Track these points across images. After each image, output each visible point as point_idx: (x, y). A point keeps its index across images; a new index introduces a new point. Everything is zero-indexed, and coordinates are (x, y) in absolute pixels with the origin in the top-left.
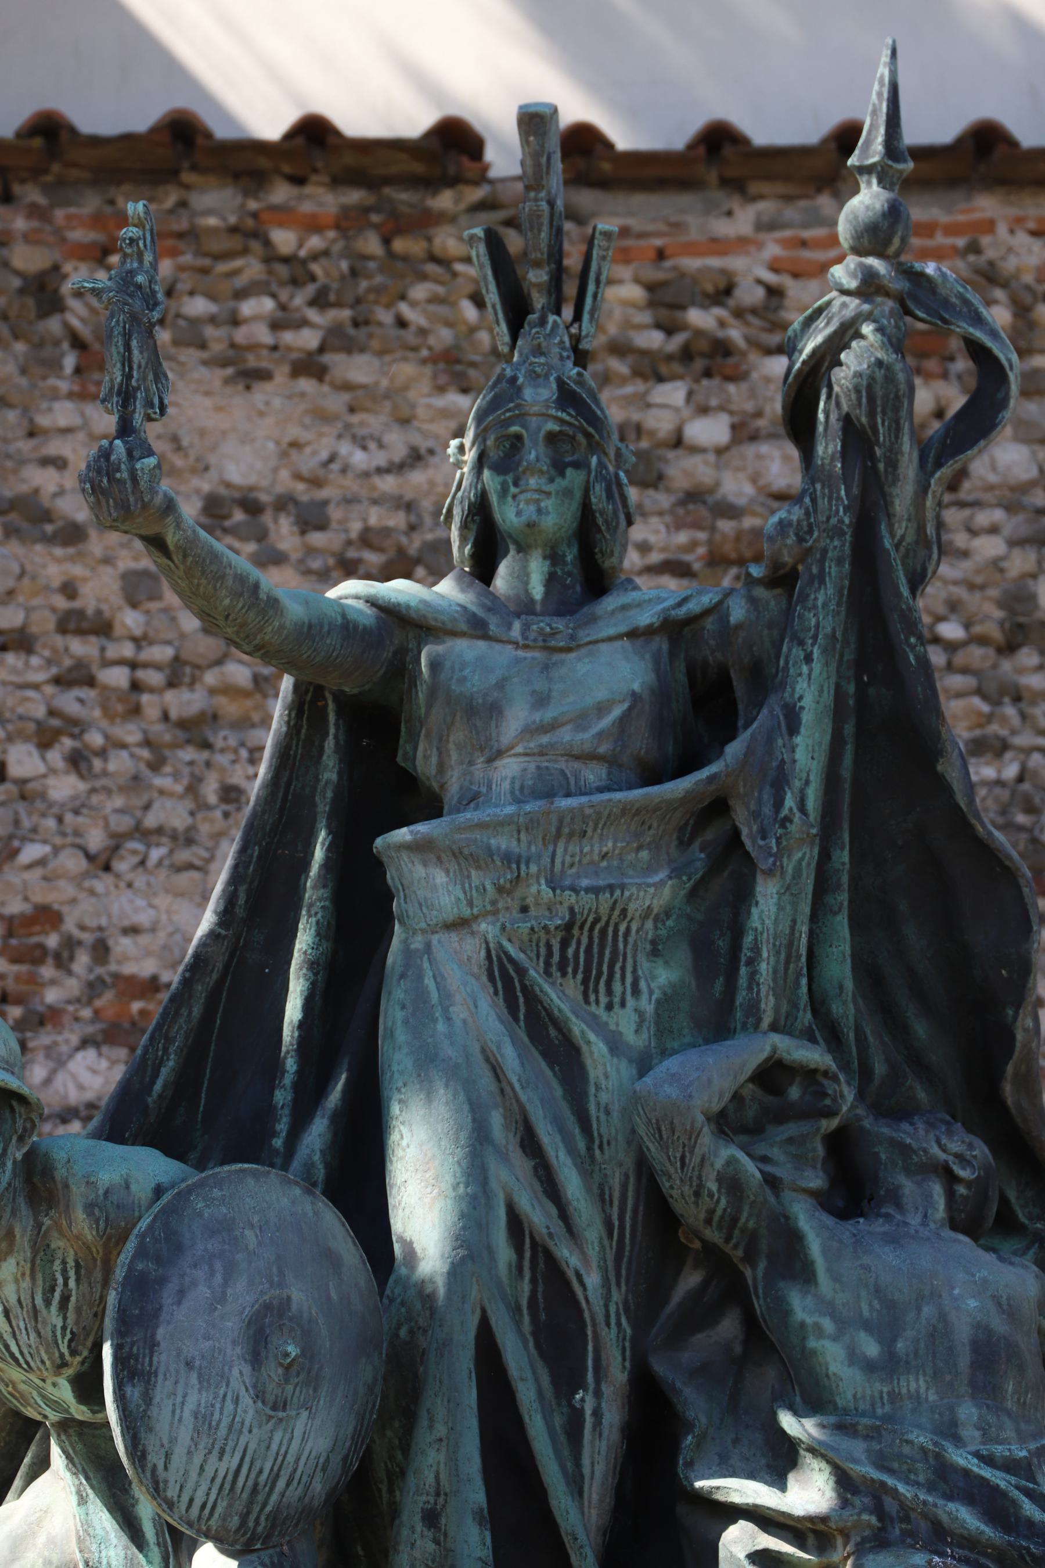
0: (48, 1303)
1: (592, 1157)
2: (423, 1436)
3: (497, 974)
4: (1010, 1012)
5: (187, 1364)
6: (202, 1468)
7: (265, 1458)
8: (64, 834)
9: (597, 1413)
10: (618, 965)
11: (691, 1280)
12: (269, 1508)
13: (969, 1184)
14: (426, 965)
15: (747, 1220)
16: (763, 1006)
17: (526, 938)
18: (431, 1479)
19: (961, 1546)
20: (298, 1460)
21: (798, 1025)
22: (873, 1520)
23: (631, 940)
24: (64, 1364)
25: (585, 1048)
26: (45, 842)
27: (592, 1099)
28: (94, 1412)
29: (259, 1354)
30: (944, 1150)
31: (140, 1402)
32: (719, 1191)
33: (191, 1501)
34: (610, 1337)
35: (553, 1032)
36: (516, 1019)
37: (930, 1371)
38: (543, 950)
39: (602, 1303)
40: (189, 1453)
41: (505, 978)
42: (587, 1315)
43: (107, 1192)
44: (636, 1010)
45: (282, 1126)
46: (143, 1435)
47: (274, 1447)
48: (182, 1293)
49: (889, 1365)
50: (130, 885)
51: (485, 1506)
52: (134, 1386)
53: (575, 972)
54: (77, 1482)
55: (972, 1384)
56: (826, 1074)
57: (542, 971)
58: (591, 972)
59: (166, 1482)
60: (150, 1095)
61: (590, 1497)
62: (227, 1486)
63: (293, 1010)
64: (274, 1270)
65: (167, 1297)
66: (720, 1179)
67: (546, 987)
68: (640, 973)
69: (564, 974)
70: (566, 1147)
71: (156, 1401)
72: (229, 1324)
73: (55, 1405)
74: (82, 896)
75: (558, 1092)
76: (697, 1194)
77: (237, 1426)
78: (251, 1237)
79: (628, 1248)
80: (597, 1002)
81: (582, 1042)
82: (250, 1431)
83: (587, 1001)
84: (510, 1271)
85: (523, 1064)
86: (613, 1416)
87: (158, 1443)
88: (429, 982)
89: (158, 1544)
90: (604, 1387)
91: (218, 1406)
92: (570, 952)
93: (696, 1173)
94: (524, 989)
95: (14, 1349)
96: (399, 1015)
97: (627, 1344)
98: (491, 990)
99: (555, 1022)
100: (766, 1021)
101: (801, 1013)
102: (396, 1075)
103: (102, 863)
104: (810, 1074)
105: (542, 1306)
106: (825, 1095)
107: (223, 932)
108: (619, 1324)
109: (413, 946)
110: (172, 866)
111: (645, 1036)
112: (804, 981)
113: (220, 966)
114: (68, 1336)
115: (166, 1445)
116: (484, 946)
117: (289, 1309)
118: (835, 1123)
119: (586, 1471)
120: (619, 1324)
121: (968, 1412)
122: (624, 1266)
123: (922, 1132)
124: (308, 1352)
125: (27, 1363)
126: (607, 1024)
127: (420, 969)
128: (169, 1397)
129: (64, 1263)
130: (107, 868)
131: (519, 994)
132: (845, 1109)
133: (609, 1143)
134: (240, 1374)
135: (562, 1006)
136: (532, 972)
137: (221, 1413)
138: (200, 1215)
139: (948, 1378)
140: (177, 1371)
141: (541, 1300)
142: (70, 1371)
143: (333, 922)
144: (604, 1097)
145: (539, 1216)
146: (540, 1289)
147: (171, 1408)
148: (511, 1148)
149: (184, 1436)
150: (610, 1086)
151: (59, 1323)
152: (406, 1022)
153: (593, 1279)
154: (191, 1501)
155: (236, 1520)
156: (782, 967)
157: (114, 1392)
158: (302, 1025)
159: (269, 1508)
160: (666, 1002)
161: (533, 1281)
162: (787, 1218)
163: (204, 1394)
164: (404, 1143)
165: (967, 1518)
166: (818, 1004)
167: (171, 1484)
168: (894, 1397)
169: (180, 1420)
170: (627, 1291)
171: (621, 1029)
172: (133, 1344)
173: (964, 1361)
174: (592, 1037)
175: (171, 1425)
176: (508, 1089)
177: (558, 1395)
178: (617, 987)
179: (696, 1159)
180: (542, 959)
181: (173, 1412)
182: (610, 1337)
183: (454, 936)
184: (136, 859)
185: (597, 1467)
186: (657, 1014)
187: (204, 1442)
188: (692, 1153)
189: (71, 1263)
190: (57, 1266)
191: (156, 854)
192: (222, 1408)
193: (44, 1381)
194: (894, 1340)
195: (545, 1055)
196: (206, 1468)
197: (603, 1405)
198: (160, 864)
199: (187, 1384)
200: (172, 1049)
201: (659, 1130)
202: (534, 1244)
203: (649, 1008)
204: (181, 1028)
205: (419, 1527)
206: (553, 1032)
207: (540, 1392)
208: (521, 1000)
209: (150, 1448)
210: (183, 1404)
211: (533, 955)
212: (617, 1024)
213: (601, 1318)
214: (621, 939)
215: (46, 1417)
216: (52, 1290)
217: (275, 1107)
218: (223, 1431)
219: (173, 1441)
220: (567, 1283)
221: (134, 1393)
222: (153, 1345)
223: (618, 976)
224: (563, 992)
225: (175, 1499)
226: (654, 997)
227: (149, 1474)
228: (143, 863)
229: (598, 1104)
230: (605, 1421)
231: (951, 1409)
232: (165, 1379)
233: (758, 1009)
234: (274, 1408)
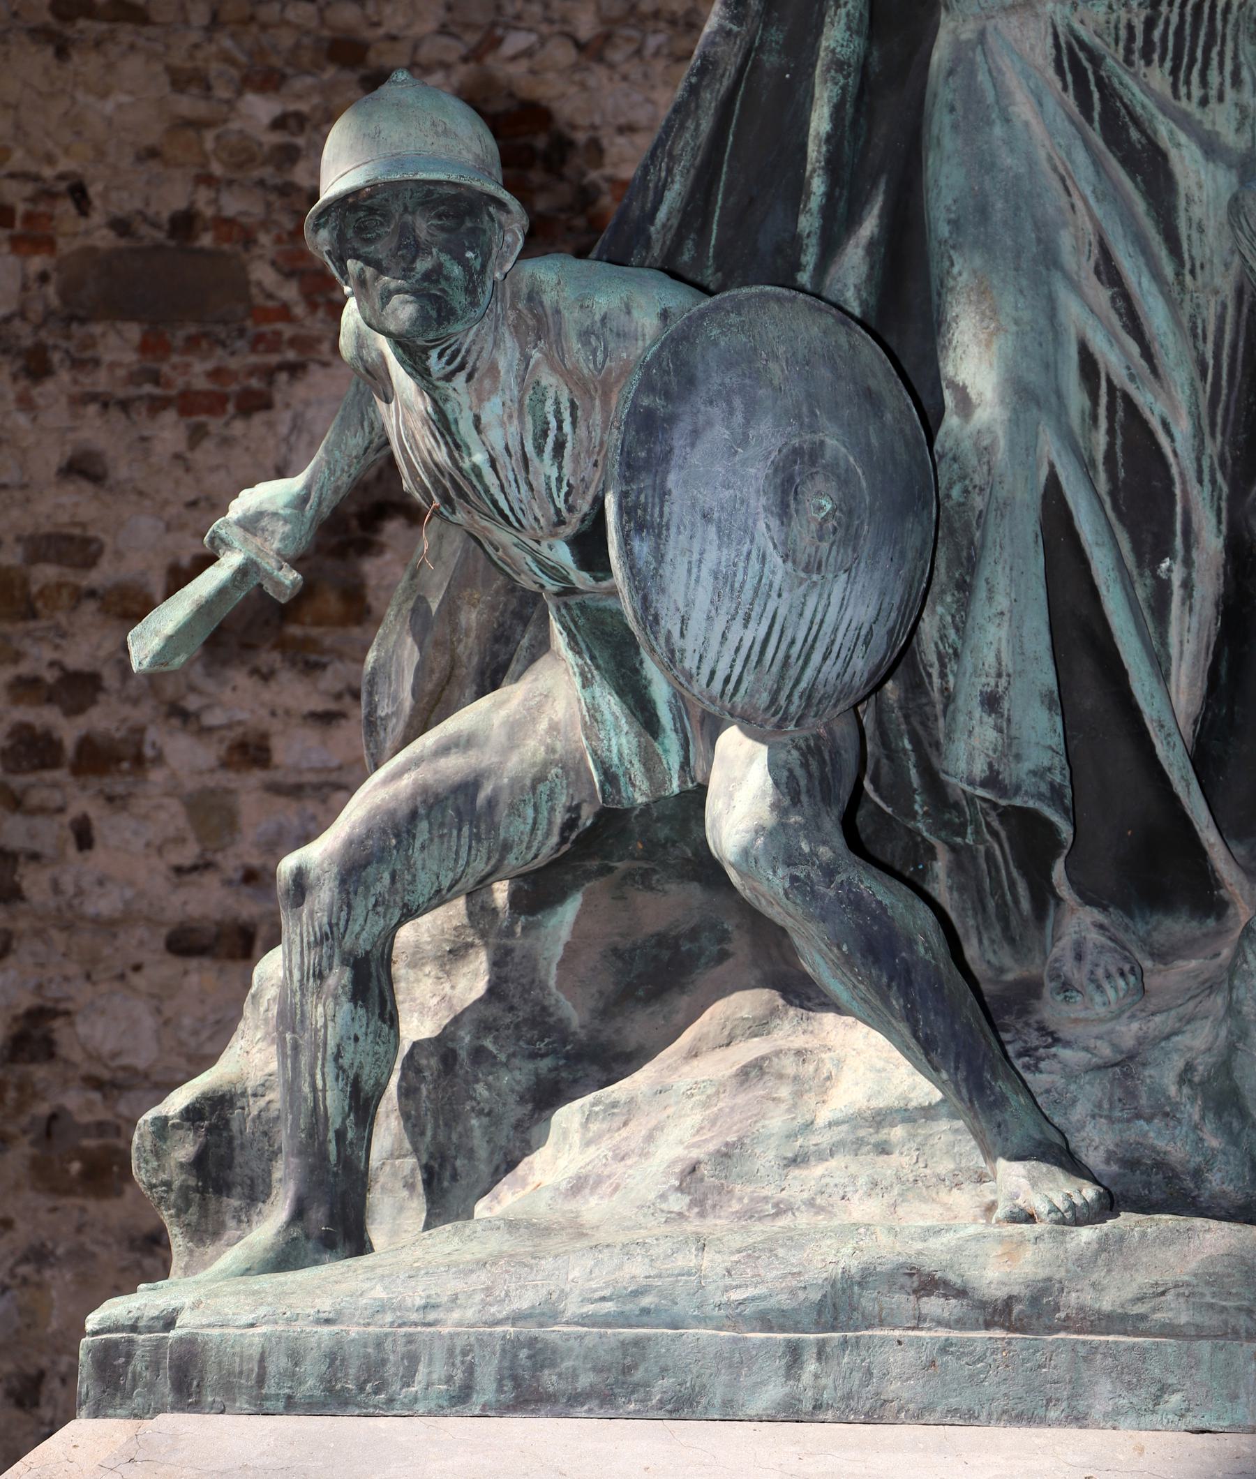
0: (540, 450)
1: (1181, 284)
2: (981, 608)
3: (1066, 64)
5: (704, 516)
6: (724, 636)
7: (797, 626)
8: (550, 21)
9: (1187, 585)
10: (1216, 50)
12: (803, 685)
14: (979, 58)
17: (1102, 18)
18: (991, 659)
20: (836, 630)
23: (1232, 18)
24: (561, 522)
25: (1173, 154)
26: (530, 30)
28: (597, 580)
29: (788, 506)
31: (651, 558)
33: (713, 673)
35: (1134, 134)
36: (1090, 120)
38: (1123, 33)
39: (1193, 456)
40: (709, 618)
41: (1076, 65)
42: (1174, 470)
43: (604, 318)
44: (1236, 105)
45: (810, 258)
46: (653, 596)
47: (808, 614)
48: (695, 434)
50: (625, 78)
51: (1055, 688)
52: (642, 540)
53: (1162, 59)
54: (580, 662)
57: (1121, 59)
58: (1181, 59)
59: (683, 651)
60: (652, 223)
62: (754, 658)
63: (820, 122)
64: (805, 410)
65: (678, 440)
67: (1127, 79)
68: (1242, 58)
69: (1149, 63)
70: (1151, 271)
71: (668, 558)
72: (752, 471)
73: (554, 572)
74: (573, 90)
77: (764, 589)
78: (776, 371)
79: (1224, 392)
80: (1189, 96)
81: (1169, 145)
82: (780, 595)
83: (1176, 96)
84: (1083, 420)
85: (1098, 173)
86: (1208, 586)
87: (672, 607)
88: (982, 77)
89: (676, 731)
91: (741, 565)
92: (1157, 34)
95: (503, 504)
96: (947, 119)
97: (1224, 505)
98: (1059, 85)
102: (944, 191)
103: (592, 51)
105: (1120, 461)
107: (735, 28)
109: (964, 37)
110: (670, 55)
113: (732, 70)
114: (565, 489)
115: (683, 610)
116: (1050, 30)
117: (823, 456)
119: (1174, 651)
120: (1213, 481)
124: (847, 509)
125: (519, 521)
126: (1200, 122)
127: (972, 62)
128: (683, 553)
129: (557, 403)
130: (600, 58)
131: (1093, 88)
133: (1202, 267)
134: (765, 528)
135: (1147, 101)
136: (1109, 61)
137: (745, 573)
138: (715, 343)
140: (693, 524)
142: (568, 531)
143: (867, 15)
144: (1197, 212)
145: (1115, 358)
146: (1119, 441)
147: (686, 566)
148: (1083, 275)
149: (703, 597)
150: (1204, 198)
151: (554, 474)
152: (955, 127)
154: (713, 673)
155: (764, 698)
157: (620, 547)
158: (832, 139)
159: (803, 685)
161: (1111, 432)
163: (725, 551)
164: (955, 270)
167: (688, 654)
169: (697, 581)
171: (1218, 128)
172: (640, 491)
174: (1182, 138)
175: (687, 586)
176: (1079, 204)
177: (1140, 564)
178: (1214, 77)
180: (1121, 45)
181: (689, 571)
183: (1014, 21)
184: (631, 48)
185: (1186, 646)
187: (727, 605)
189: (565, 404)
190: (549, 407)
191: (653, 42)
192: (746, 568)
193: (538, 542)
195: (1124, 162)
196: (729, 636)
197: (1194, 575)
198: (657, 54)
199: (704, 540)
200: (677, 170)
204: (687, 143)
205: (978, 712)
206: (1134, 134)
207: (1120, 559)
208: (1096, 96)
209: (663, 613)
210: (700, 561)
211: (1111, 40)
212: (1214, 123)
213: (1191, 475)
214: (1219, 16)
215: (542, 586)
216: (545, 434)
217: (800, 237)
218: (748, 594)
219: (689, 604)
220: (1151, 434)
221: (642, 548)
222: (664, 494)
223: (1215, 63)
224: (1147, 84)
225: (694, 671)
227: (662, 641)
228: (638, 52)
229: (1190, 219)
230: (1196, 594)
232: (679, 533)
234: (807, 569)
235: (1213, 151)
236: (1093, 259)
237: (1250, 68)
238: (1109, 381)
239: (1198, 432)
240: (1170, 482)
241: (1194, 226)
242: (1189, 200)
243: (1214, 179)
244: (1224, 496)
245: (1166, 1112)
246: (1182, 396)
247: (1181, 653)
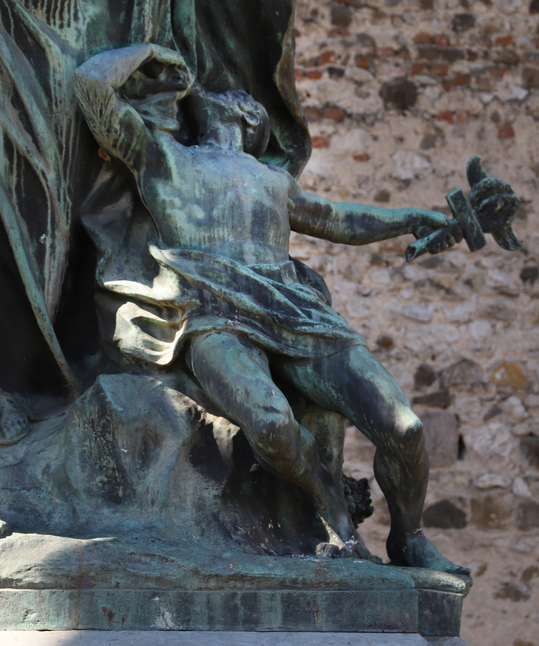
4: (280, 35)
9: (53, 246)
11: (105, 177)
13: (254, 128)
15: (136, 146)
16: (146, 28)
19: (242, 315)
21: (165, 39)
22: (198, 302)
25: (47, 49)
27: (51, 78)
30: (242, 109)
32: (120, 129)
34: (60, 206)
35: (30, 40)
36: (9, 32)
37: (230, 226)
39: (56, 188)
42: (48, 195)
44: (76, 29)
49: (210, 223)
55: (252, 232)
56: (180, 67)
57: (23, 4)
58: (51, 6)
61: (48, 290)
66: (121, 123)
67: (26, 14)
68: (78, 8)
69: (36, 7)
75: (33, 73)
76: (109, 131)
79: (70, 159)
80: (55, 24)
83: (49, 22)
84: (6, 170)
85: (13, 57)
86: (61, 248)
90: (56, 233)
93: (108, 119)
94: (14, 14)
97: (70, 211)
99: (31, 34)
100: (148, 37)
101: (167, 33)
104: (171, 67)
105: (23, 189)
106: (179, 78)
108: (65, 200)
111: (81, 43)
112: (169, 15)
118: (184, 94)
119: (46, 276)
120: (65, 200)
121: (249, 247)
122: (68, 169)
123: (230, 100)
131: (11, 17)
132: (189, 86)
133: (60, 102)
135: (35, 25)
136: (18, 5)
139: (240, 229)
141: (22, 186)
144: (58, 77)
145: (22, 141)
146: (22, 180)
148: (6, 103)
150: (62, 71)
153: (51, 176)
156: (157, 7)
160: (93, 25)
161: (19, 176)
162: (157, 145)
165: (246, 300)
166: (176, 28)
168: (211, 239)
170: (70, 182)
171: (68, 39)
173: (248, 221)
174: (51, 43)
177: (31, 236)
178: (66, 15)
179: (108, 112)
182: (60, 206)
185: (52, 274)
186: (88, 31)
188: (106, 108)
194: (212, 209)
197: (56, 242)
201: (88, 95)
202: (19, 156)
203: (83, 28)
206: (30, 40)
207: (22, 235)
208: (12, 21)
212: (66, 36)
220: (37, 177)
223: (66, 9)
224: (35, 17)
226: (86, 22)
229: (55, 80)
230: (57, 251)
231: (241, 245)
233: (143, 30)
235: (65, 49)
236: (11, 96)
237: (82, 12)
238: (18, 153)
239: (58, 178)
240: (46, 200)
241: (57, 83)
242: (55, 71)
243: (66, 62)
244: (70, 207)
245: (37, 487)
246: (51, 161)
247: (50, 277)
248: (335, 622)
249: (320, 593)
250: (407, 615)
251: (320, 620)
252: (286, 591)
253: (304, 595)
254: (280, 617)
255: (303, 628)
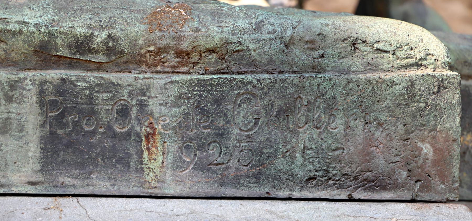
248: (203, 167)
249: (159, 81)
250: (427, 149)
251: (159, 162)
252: (54, 74)
253: (111, 87)
254: (34, 150)
255: (102, 186)
